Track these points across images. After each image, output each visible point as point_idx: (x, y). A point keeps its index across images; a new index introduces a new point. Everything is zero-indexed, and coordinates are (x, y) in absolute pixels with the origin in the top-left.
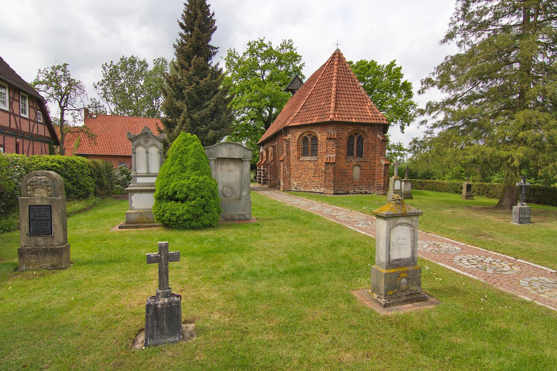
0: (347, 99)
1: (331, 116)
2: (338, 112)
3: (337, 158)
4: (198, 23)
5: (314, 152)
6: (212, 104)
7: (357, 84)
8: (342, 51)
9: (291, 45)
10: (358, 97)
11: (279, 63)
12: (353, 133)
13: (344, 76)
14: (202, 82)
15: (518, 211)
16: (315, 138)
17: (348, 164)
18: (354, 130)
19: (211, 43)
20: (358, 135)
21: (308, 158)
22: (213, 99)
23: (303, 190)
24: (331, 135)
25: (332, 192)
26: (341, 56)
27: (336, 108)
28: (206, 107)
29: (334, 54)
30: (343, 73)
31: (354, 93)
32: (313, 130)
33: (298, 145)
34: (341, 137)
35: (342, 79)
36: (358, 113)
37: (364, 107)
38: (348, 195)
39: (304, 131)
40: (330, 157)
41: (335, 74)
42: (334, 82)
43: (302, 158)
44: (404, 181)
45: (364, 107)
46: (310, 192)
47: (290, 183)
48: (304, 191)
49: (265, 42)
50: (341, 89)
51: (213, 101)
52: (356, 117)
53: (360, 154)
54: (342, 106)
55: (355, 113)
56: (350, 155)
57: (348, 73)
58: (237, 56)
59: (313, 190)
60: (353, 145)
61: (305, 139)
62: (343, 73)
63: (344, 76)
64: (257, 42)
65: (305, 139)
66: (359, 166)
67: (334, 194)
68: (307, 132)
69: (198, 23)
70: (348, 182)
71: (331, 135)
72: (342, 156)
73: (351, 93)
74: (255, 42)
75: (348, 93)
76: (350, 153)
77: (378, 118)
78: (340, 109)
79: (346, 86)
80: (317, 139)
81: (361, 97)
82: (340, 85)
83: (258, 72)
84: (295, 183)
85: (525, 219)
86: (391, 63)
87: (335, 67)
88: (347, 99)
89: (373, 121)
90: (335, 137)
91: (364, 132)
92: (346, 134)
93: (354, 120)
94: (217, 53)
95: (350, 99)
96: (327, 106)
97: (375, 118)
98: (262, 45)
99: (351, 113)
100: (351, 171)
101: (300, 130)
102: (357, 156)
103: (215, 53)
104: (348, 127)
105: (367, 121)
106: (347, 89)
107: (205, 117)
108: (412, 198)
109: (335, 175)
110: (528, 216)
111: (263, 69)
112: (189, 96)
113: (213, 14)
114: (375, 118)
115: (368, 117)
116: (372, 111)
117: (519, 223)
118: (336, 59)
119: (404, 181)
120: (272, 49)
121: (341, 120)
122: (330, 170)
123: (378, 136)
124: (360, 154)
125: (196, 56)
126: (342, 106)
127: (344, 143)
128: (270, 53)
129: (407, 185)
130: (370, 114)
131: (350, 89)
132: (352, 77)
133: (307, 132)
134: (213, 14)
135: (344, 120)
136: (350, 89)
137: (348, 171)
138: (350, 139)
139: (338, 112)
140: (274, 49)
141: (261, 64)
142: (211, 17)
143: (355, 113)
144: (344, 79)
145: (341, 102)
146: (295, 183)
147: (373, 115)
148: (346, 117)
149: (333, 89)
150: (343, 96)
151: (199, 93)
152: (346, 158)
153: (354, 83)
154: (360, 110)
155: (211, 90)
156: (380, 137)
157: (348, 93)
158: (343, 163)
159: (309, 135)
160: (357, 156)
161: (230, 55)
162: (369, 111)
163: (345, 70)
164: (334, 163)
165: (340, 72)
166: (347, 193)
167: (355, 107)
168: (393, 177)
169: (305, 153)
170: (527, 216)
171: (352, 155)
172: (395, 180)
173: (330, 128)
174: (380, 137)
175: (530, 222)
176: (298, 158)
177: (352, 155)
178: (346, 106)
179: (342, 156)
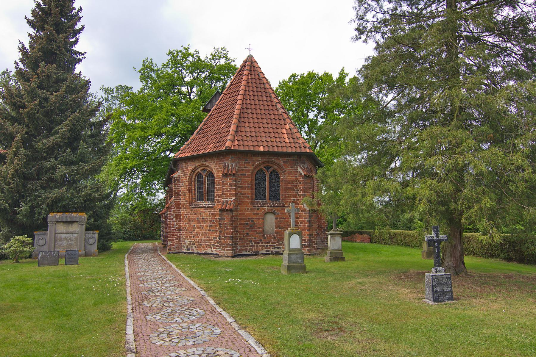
0: (256, 120)
1: (228, 144)
3: (239, 202)
4: (55, 22)
5: (211, 196)
6: (65, 128)
7: (273, 99)
8: (256, 58)
10: (273, 117)
11: (211, 78)
12: (262, 166)
13: (255, 89)
14: (52, 98)
15: (430, 281)
16: (211, 175)
17: (256, 211)
19: (77, 48)
20: (271, 170)
21: (202, 204)
22: (66, 122)
23: (196, 251)
24: (228, 170)
25: (230, 253)
26: (255, 64)
27: (236, 131)
28: (57, 132)
29: (245, 62)
30: (255, 85)
31: (267, 112)
32: (207, 163)
33: (190, 184)
35: (251, 93)
36: (268, 139)
37: (279, 131)
39: (197, 164)
40: (227, 201)
41: (242, 88)
42: (239, 97)
43: (195, 204)
44: (331, 234)
45: (279, 131)
46: (205, 254)
47: (180, 240)
48: (198, 253)
49: (191, 51)
50: (249, 106)
51: (67, 125)
52: (265, 144)
53: (275, 196)
54: (248, 129)
55: (264, 139)
56: (260, 198)
57: (262, 86)
58: (156, 68)
59: (209, 251)
60: (264, 183)
61: (199, 176)
62: (255, 85)
63: (255, 89)
64: (181, 52)
65: (199, 176)
66: (274, 213)
67: (232, 257)
69: (55, 22)
70: (258, 237)
71: (228, 170)
72: (246, 199)
73: (263, 112)
75: (258, 111)
76: (259, 195)
77: (297, 145)
79: (257, 102)
80: (213, 176)
81: (277, 117)
82: (248, 102)
83: (184, 89)
84: (187, 241)
85: (443, 293)
86: (340, 74)
87: (244, 78)
88: (256, 120)
89: (290, 150)
90: (234, 172)
91: (278, 165)
92: (251, 167)
93: (261, 149)
94: (84, 60)
96: (227, 129)
97: (293, 145)
98: (186, 55)
99: (259, 139)
100: (261, 221)
101: (192, 163)
102: (270, 199)
103: (80, 60)
104: (255, 158)
105: (280, 150)
106: (258, 107)
108: (343, 259)
109: (234, 227)
110: (449, 289)
111: (191, 85)
112: (29, 117)
113: (80, 10)
114: (293, 145)
116: (290, 136)
117: (434, 301)
118: (247, 68)
119: (331, 234)
120: (199, 59)
121: (242, 148)
122: (227, 221)
123: (299, 170)
124: (275, 196)
125: (43, 63)
126: (248, 129)
127: (248, 181)
128: (198, 66)
129: (334, 240)
131: (262, 107)
132: (267, 91)
134: (80, 10)
135: (247, 149)
136: (262, 107)
137: (256, 221)
138: (259, 174)
140: (203, 60)
141: (187, 79)
142: (77, 13)
143: (264, 139)
144: (256, 93)
145: (247, 124)
146: (187, 241)
147: (292, 140)
148: (250, 143)
149: (237, 107)
150: (250, 116)
151: (48, 114)
152: (253, 203)
153: (269, 99)
154: (272, 135)
155: (69, 109)
156: (302, 172)
157: (258, 111)
158: (247, 210)
159: (204, 170)
160: (270, 199)
161: (145, 67)
162: (286, 136)
163: (258, 81)
164: (231, 210)
165: (250, 84)
166: (257, 254)
167: (266, 130)
168: (289, 230)
170: (446, 289)
172: (291, 234)
173: (227, 160)
174: (302, 172)
175: (452, 299)
176: (190, 204)
177: (263, 197)
178: (253, 129)
179: (246, 199)
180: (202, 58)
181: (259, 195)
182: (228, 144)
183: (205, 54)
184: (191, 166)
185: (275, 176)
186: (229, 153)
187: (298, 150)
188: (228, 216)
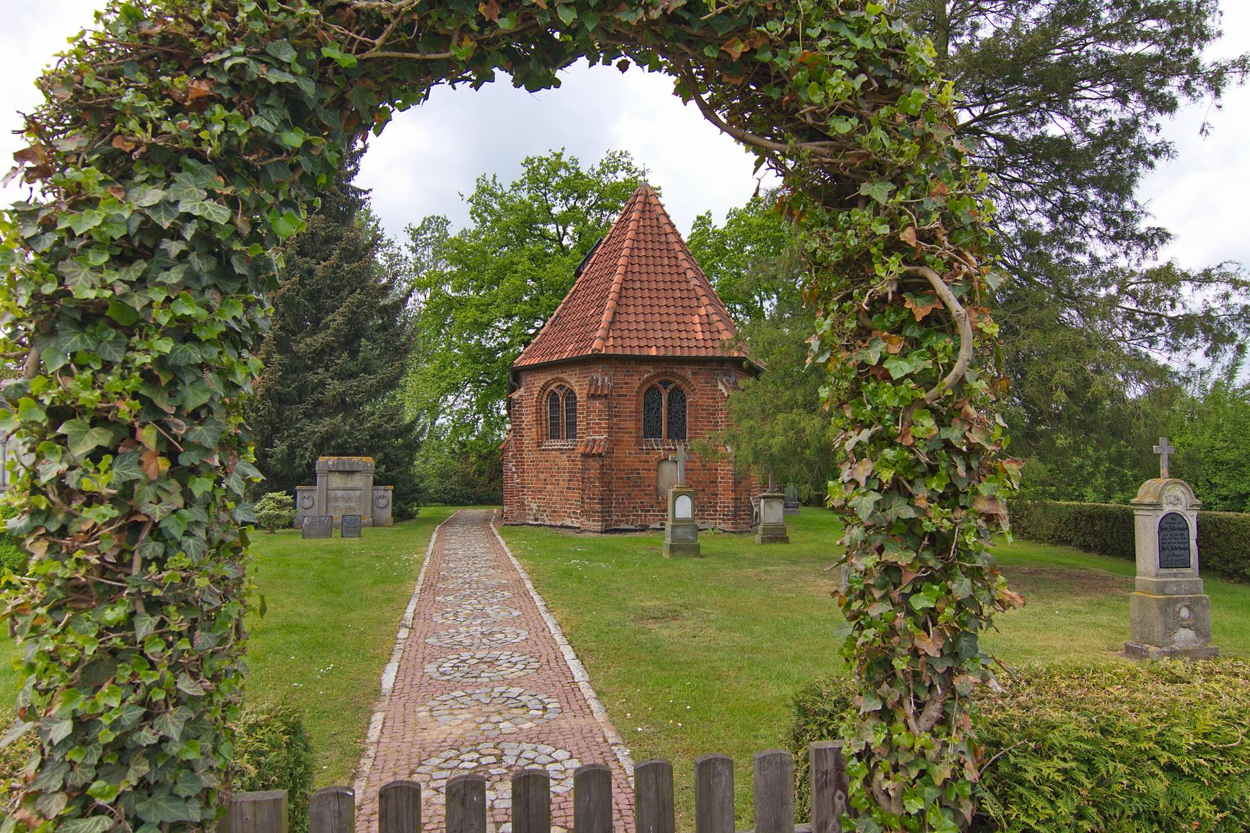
0: (647, 302)
1: (597, 344)
2: (618, 333)
3: (614, 443)
6: (340, 319)
7: (680, 262)
9: (629, 164)
10: (678, 294)
13: (650, 245)
16: (571, 396)
17: (644, 457)
18: (658, 375)
19: (357, 182)
20: (671, 387)
21: (557, 444)
22: (341, 309)
23: (548, 523)
24: (597, 387)
25: (598, 526)
26: (652, 200)
27: (612, 322)
28: (327, 326)
31: (669, 285)
34: (624, 391)
35: (643, 253)
36: (667, 334)
37: (687, 319)
38: (643, 534)
39: (549, 378)
40: (594, 441)
41: (627, 243)
42: (622, 261)
44: (764, 497)
45: (687, 319)
46: (562, 527)
47: (523, 504)
48: (551, 526)
49: (565, 159)
50: (637, 277)
51: (342, 314)
52: (661, 342)
55: (659, 334)
56: (653, 435)
57: (663, 239)
58: (499, 192)
59: (568, 522)
62: (649, 238)
63: (650, 245)
68: (555, 380)
70: (647, 501)
71: (597, 387)
72: (626, 437)
73: (661, 285)
74: (541, 160)
75: (653, 285)
76: (651, 430)
77: (717, 344)
78: (624, 326)
81: (685, 294)
82: (636, 268)
83: (552, 229)
84: (534, 506)
87: (632, 225)
88: (647, 302)
89: (703, 353)
91: (683, 379)
92: (635, 382)
93: (653, 352)
95: (655, 302)
97: (709, 344)
101: (541, 376)
104: (642, 368)
106: (653, 277)
107: (322, 350)
108: (785, 540)
109: (607, 484)
111: (563, 221)
114: (709, 344)
115: (693, 343)
116: (706, 327)
118: (638, 207)
119: (764, 497)
121: (619, 351)
123: (721, 387)
126: (632, 318)
127: (629, 406)
128: (576, 185)
129: (771, 507)
130: (700, 336)
131: (660, 278)
132: (671, 247)
133: (555, 380)
136: (660, 278)
137: (644, 474)
139: (618, 333)
143: (659, 334)
144: (650, 253)
145: (631, 309)
146: (534, 506)
147: (708, 335)
148: (635, 343)
149: (617, 278)
151: (313, 296)
152: (638, 443)
153: (673, 262)
154: (675, 326)
156: (724, 391)
157: (653, 285)
158: (629, 455)
159: (561, 387)
161: (482, 190)
162: (698, 328)
163: (656, 230)
164: (600, 455)
165: (642, 236)
166: (644, 529)
167: (665, 318)
171: (658, 433)
173: (596, 371)
174: (724, 391)
176: (539, 444)
177: (658, 433)
178: (641, 318)
179: (626, 437)
180: (584, 170)
181: (651, 430)
182: (597, 344)
183: (589, 164)
184: (540, 381)
185: (678, 398)
186: (597, 359)
187: (719, 353)
188: (595, 464)
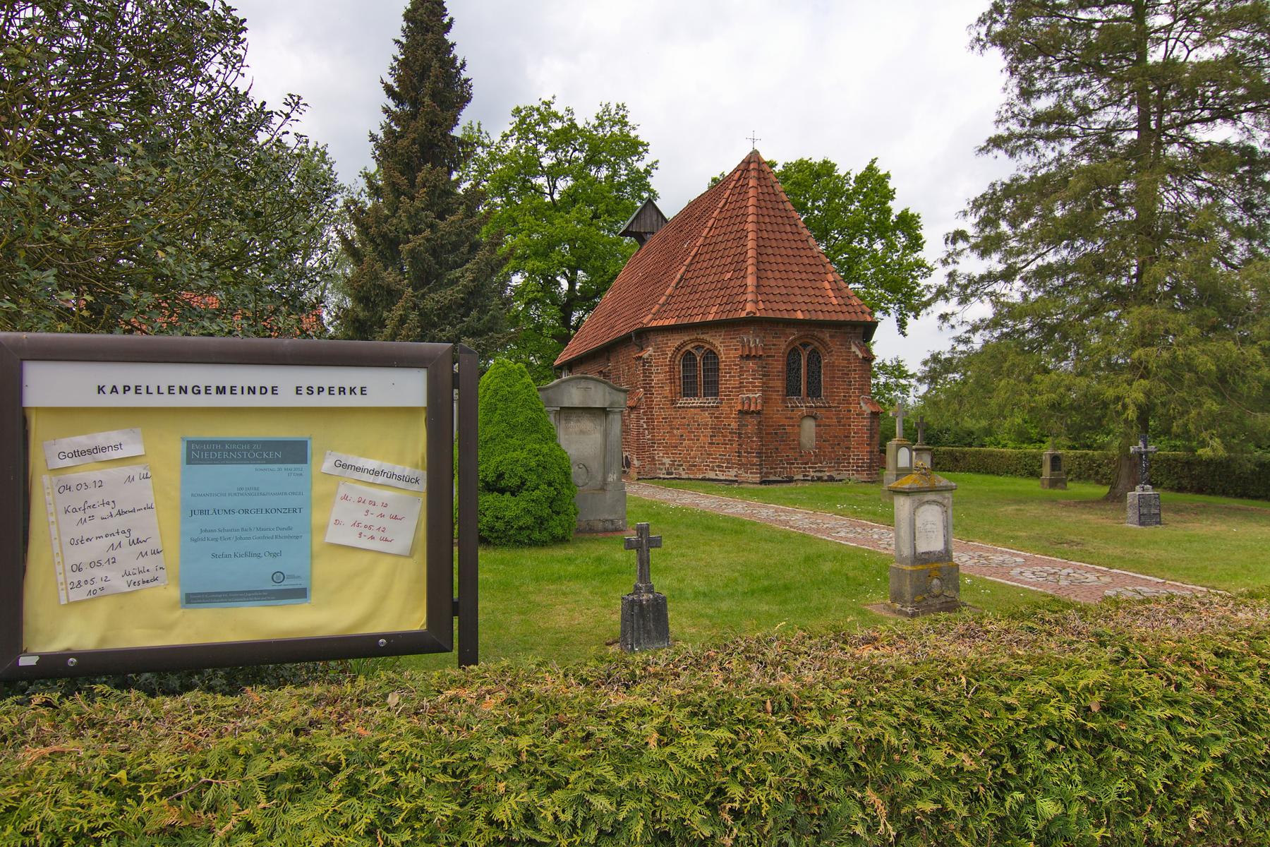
1: (749, 307)
2: (765, 297)
3: (766, 400)
5: (712, 388)
7: (801, 230)
9: (624, 117)
11: (592, 160)
12: (797, 343)
15: (1136, 501)
16: (711, 356)
17: (789, 414)
18: (800, 338)
20: (810, 348)
21: (696, 402)
25: (757, 478)
27: (757, 287)
28: (454, 282)
33: (672, 370)
34: (772, 352)
37: (818, 284)
38: (792, 485)
39: (686, 338)
43: (682, 402)
44: (916, 450)
45: (818, 284)
46: (703, 479)
49: (558, 108)
53: (814, 391)
57: (781, 207)
58: (487, 141)
59: (712, 475)
60: (799, 369)
64: (538, 109)
65: (689, 357)
66: (815, 418)
67: (761, 483)
68: (692, 341)
70: (791, 454)
72: (774, 396)
74: (532, 109)
77: (851, 310)
78: (767, 290)
82: (765, 235)
83: (541, 181)
84: (667, 461)
87: (751, 192)
91: (822, 341)
92: (782, 345)
93: (800, 315)
95: (788, 267)
97: (845, 309)
98: (547, 116)
99: (793, 299)
100: (796, 430)
101: (676, 336)
102: (808, 395)
104: (788, 331)
107: (449, 308)
111: (553, 173)
114: (845, 309)
115: (830, 308)
116: (837, 293)
118: (753, 174)
119: (916, 450)
120: (575, 126)
123: (854, 349)
124: (814, 391)
125: (429, 165)
126: (772, 283)
127: (778, 366)
128: (567, 136)
130: (834, 301)
133: (692, 341)
134: (463, 65)
138: (793, 354)
139: (765, 297)
140: (580, 126)
141: (546, 162)
142: (458, 72)
143: (800, 299)
146: (667, 461)
147: (842, 302)
149: (750, 244)
152: (784, 401)
155: (463, 243)
156: (858, 352)
158: (777, 412)
159: (697, 348)
162: (831, 293)
164: (759, 413)
165: (763, 204)
166: (790, 480)
167: (801, 284)
169: (689, 389)
170: (1154, 511)
171: (797, 392)
172: (899, 447)
174: (858, 352)
176: (673, 402)
177: (797, 392)
179: (774, 396)
182: (749, 307)
183: (585, 117)
184: (675, 341)
185: (815, 359)
186: (751, 322)
187: (855, 318)
188: (752, 421)
